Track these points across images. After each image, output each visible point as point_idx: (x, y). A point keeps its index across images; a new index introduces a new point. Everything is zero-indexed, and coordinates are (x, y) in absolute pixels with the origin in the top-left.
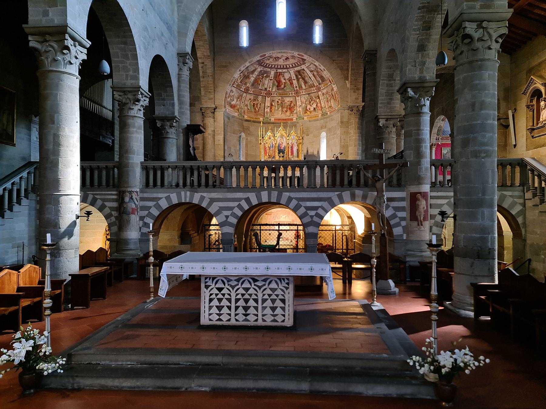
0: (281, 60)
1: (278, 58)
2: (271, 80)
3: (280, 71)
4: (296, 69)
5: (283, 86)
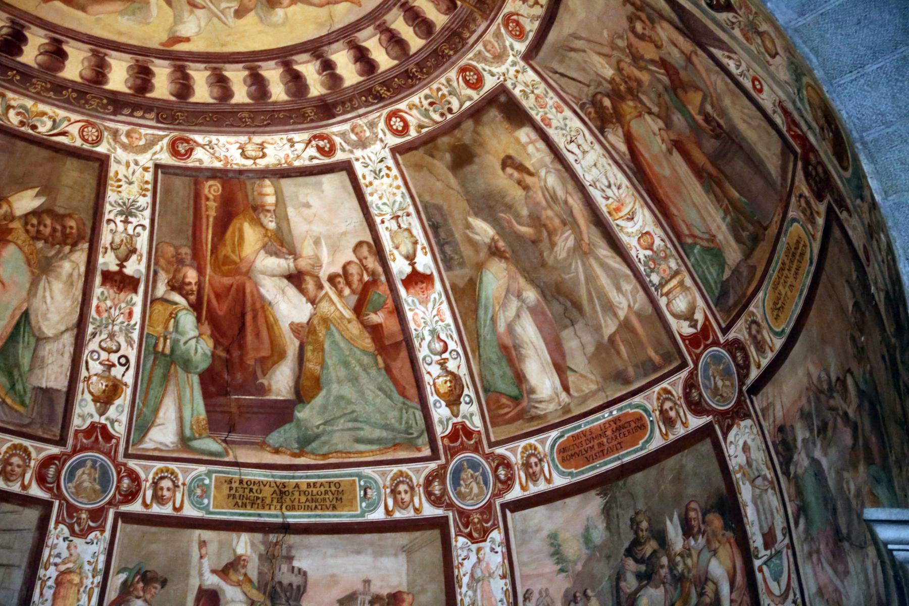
2: (121, 282)
3: (221, 150)
4: (417, 110)
5: (281, 381)
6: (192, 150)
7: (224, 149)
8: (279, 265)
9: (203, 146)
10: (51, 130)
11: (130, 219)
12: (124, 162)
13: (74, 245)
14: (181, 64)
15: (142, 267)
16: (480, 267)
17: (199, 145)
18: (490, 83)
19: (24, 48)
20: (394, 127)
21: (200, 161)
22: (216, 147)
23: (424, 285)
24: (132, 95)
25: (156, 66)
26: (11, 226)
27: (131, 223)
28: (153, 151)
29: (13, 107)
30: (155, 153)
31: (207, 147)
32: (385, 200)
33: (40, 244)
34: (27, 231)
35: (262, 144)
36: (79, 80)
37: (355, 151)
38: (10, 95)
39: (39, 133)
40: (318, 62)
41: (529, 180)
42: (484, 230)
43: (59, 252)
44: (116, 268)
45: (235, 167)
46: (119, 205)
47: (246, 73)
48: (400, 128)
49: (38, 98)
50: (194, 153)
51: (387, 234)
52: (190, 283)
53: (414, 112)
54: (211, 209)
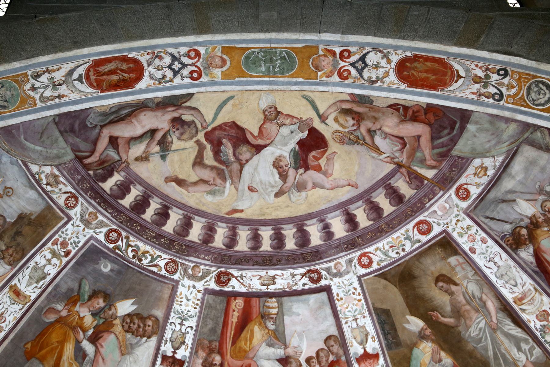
0: (261, 169)
1: (238, 135)
6: (229, 280)
7: (249, 280)
8: (274, 353)
9: (236, 278)
10: (149, 263)
11: (184, 322)
12: (187, 286)
13: (149, 337)
14: (234, 225)
15: (187, 354)
16: (412, 346)
17: (234, 277)
18: (436, 230)
19: (147, 210)
20: (363, 263)
21: (233, 287)
22: (244, 278)
23: (371, 361)
24: (200, 244)
25: (219, 227)
26: (114, 322)
27: (184, 325)
28: (205, 280)
29: (132, 246)
30: (206, 282)
31: (239, 278)
32: (349, 309)
33: (129, 336)
34: (123, 326)
35: (274, 277)
36: (172, 233)
37: (334, 279)
38: (132, 238)
39: (142, 264)
40: (321, 224)
41: (453, 288)
42: (415, 324)
43: (139, 341)
44: (171, 354)
45: (254, 291)
46: (179, 313)
47: (272, 232)
48: (367, 264)
49: (147, 240)
50: (231, 282)
51: (349, 330)
52: (216, 364)
53: (378, 252)
54: (234, 318)
